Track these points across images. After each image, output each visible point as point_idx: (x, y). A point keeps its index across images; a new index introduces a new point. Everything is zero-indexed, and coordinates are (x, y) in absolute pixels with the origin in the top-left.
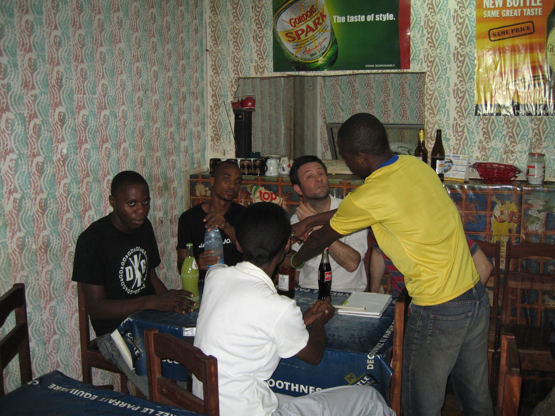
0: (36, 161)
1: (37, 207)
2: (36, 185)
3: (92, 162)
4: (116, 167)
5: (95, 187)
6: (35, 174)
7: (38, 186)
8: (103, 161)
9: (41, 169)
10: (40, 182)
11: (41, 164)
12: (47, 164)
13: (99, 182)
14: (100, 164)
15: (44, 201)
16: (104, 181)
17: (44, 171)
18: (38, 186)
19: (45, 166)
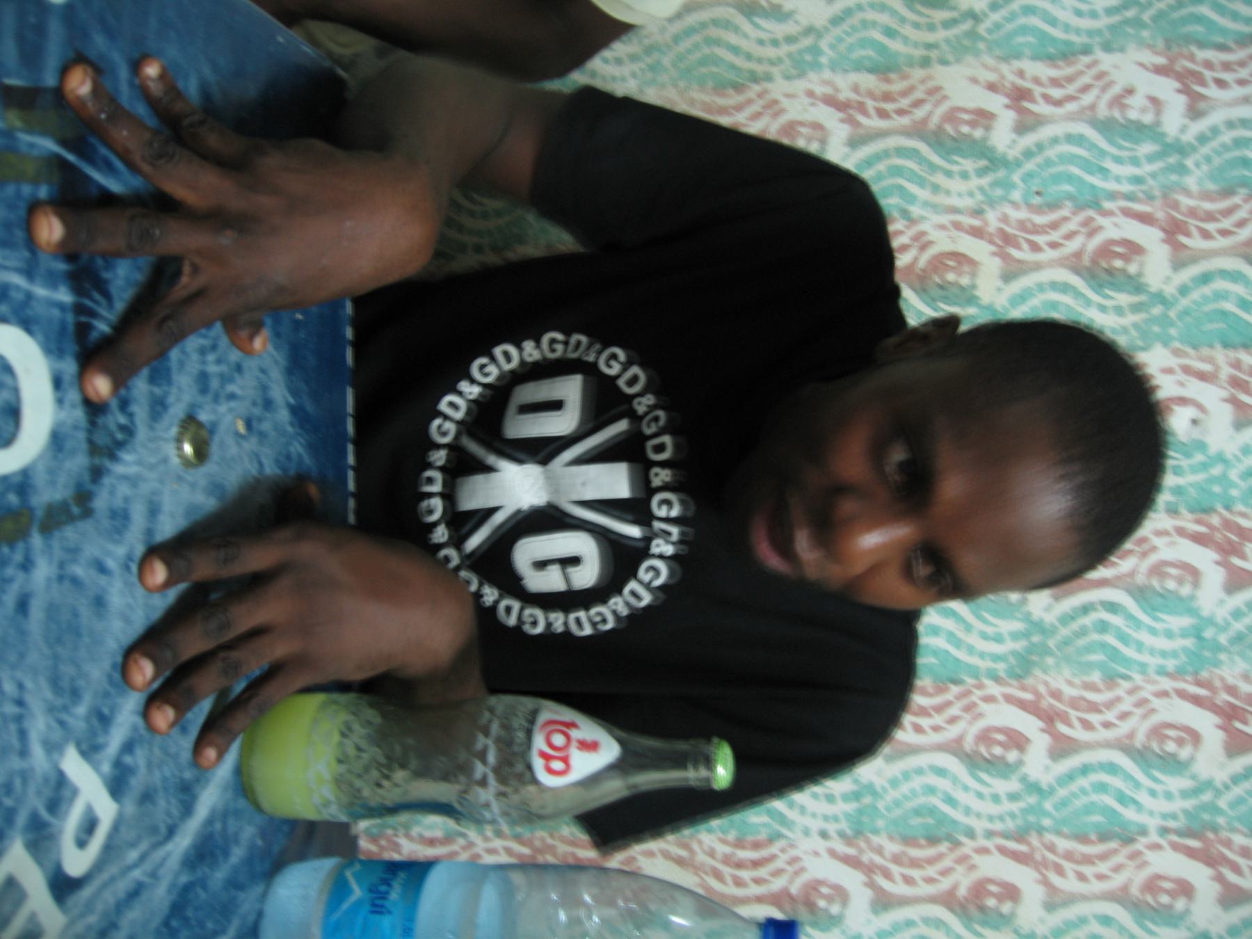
0: (1149, 237)
1: (943, 243)
2: (1040, 240)
3: (1130, 617)
4: (1089, 809)
5: (998, 639)
6: (1091, 234)
7: (1035, 247)
8: (1125, 706)
9: (1110, 272)
10: (1051, 264)
11: (1132, 269)
12: (1136, 308)
13: (1023, 666)
14: (1111, 680)
15: (965, 281)
16: (1022, 705)
17: (1098, 287)
18: (1035, 247)
19: (1124, 299)
